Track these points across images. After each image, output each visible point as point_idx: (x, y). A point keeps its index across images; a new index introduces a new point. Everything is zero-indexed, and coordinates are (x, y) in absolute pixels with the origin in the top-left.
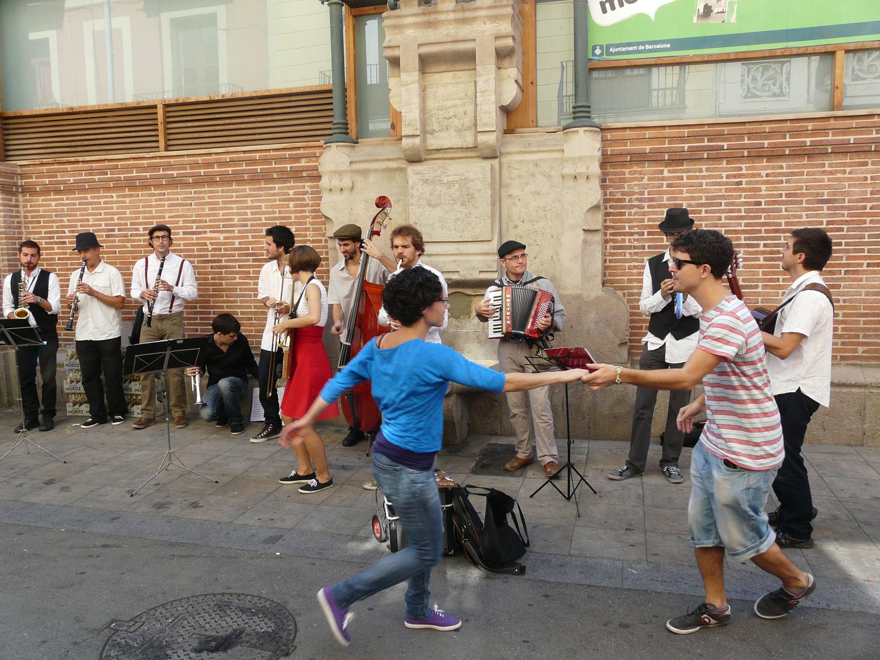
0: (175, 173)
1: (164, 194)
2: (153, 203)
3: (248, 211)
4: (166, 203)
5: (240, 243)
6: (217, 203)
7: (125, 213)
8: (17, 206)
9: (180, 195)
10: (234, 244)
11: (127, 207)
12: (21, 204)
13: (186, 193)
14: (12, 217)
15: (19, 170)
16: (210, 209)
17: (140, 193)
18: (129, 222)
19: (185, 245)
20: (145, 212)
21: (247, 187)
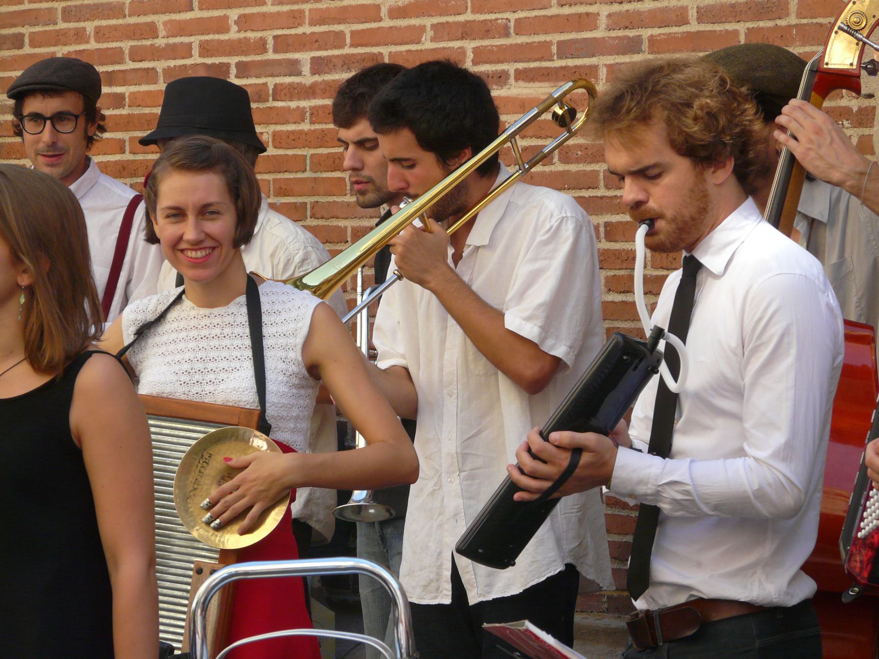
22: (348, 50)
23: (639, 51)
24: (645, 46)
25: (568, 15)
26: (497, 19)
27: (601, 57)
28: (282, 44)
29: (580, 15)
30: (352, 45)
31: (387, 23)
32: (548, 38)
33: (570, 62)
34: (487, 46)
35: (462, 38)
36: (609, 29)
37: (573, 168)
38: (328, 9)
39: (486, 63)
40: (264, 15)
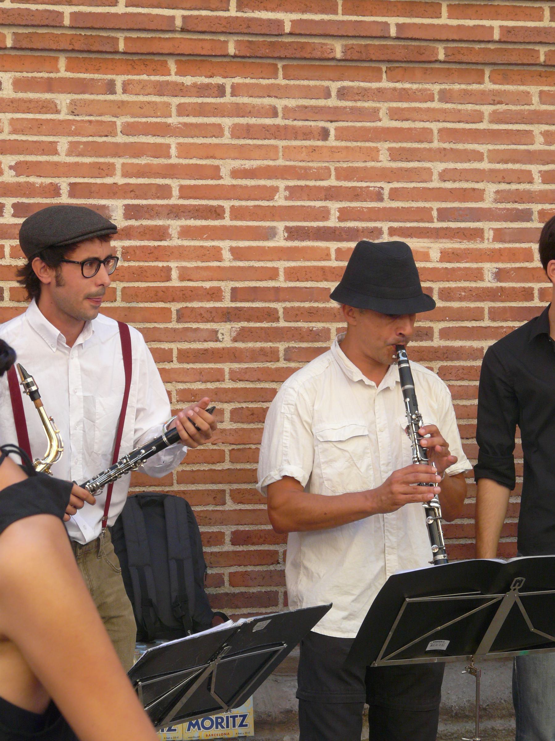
0: (288, 19)
1: (221, 91)
2: (174, 120)
3: (535, 169)
4: (227, 122)
5: (500, 275)
6: (424, 135)
7: (52, 149)
9: (282, 97)
10: (478, 275)
11: (60, 128)
13: (308, 93)
16: (395, 155)
17: (119, 80)
18: (64, 184)
19: (291, 274)
20: (137, 150)
21: (534, 90)
22: (174, 201)
23: (529, 220)
24: (535, 216)
25: (452, 189)
26: (369, 187)
27: (487, 223)
29: (465, 190)
30: (181, 197)
31: (227, 181)
32: (427, 205)
33: (453, 225)
34: (357, 207)
35: (326, 199)
36: (496, 201)
37: (456, 305)
38: (147, 165)
39: (355, 220)
40: (56, 164)
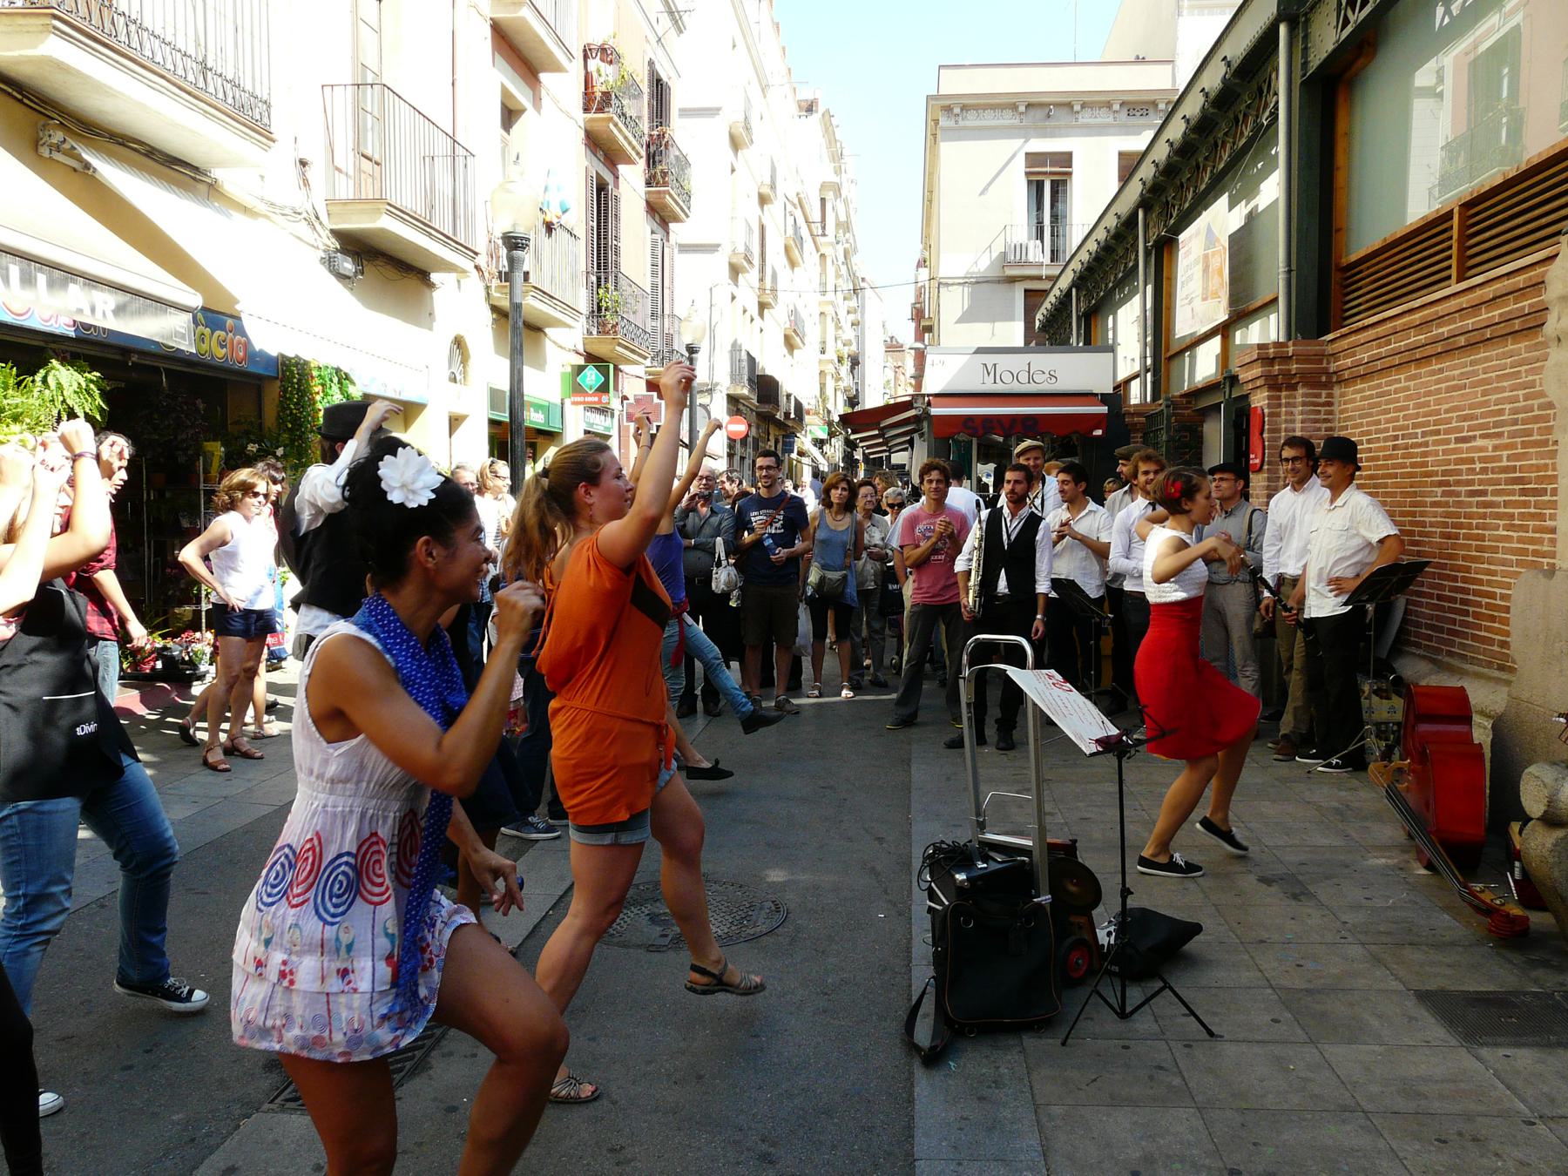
1: (1441, 371)
8: (1329, 404)
9: (1454, 368)
12: (1336, 401)
14: (1316, 421)
15: (1330, 349)
28: (1415, 426)
